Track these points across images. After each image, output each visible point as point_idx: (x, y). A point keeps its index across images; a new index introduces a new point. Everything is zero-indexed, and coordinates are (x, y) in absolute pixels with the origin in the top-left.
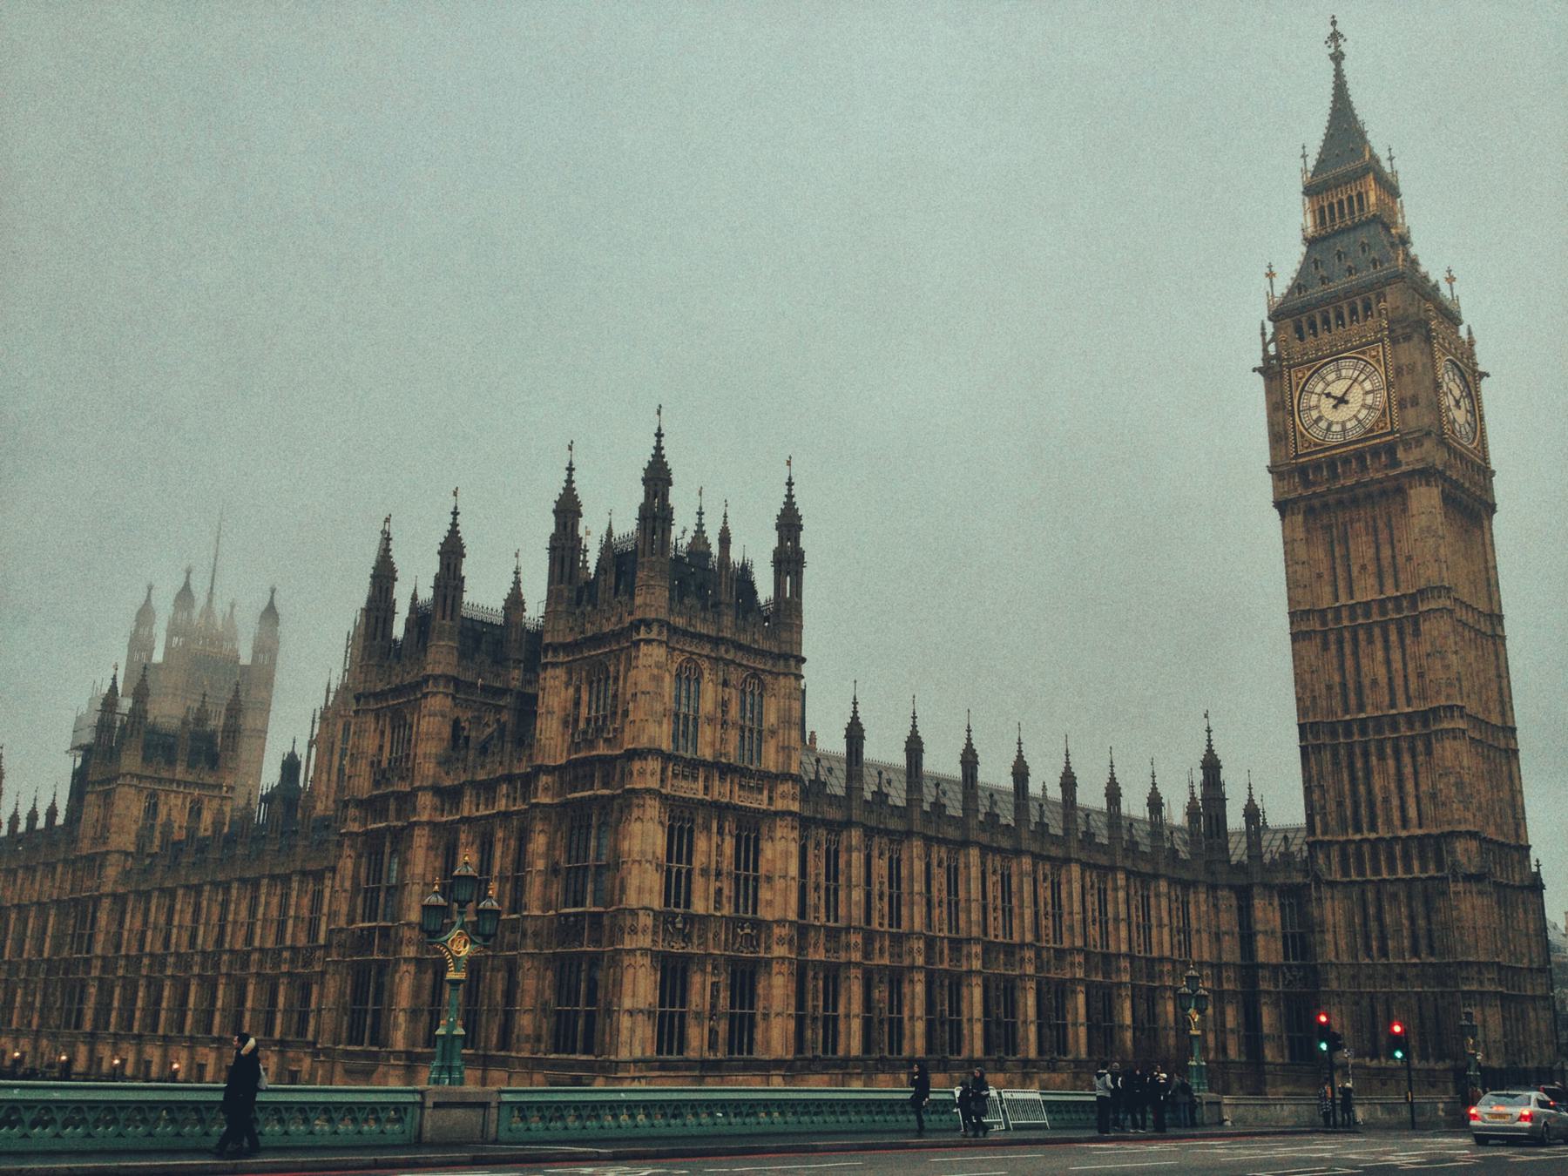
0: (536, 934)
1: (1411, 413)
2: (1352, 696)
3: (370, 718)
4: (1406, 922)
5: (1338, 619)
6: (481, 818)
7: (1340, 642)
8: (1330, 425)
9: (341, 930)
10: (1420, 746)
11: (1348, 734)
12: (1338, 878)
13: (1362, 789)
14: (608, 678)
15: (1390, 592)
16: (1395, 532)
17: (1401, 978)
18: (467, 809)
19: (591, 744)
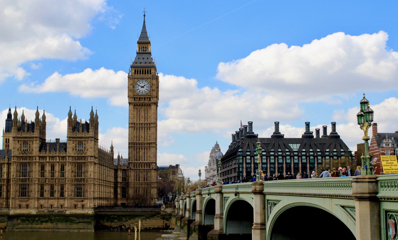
0: (70, 181)
1: (154, 92)
2: (138, 139)
3: (17, 141)
4: (143, 176)
5: (137, 125)
6: (51, 162)
7: (137, 129)
8: (140, 91)
9: (15, 178)
10: (148, 148)
11: (137, 145)
12: (133, 168)
13: (138, 154)
14: (82, 144)
15: (146, 122)
16: (148, 112)
17: (142, 184)
18: (48, 160)
19: (82, 154)
